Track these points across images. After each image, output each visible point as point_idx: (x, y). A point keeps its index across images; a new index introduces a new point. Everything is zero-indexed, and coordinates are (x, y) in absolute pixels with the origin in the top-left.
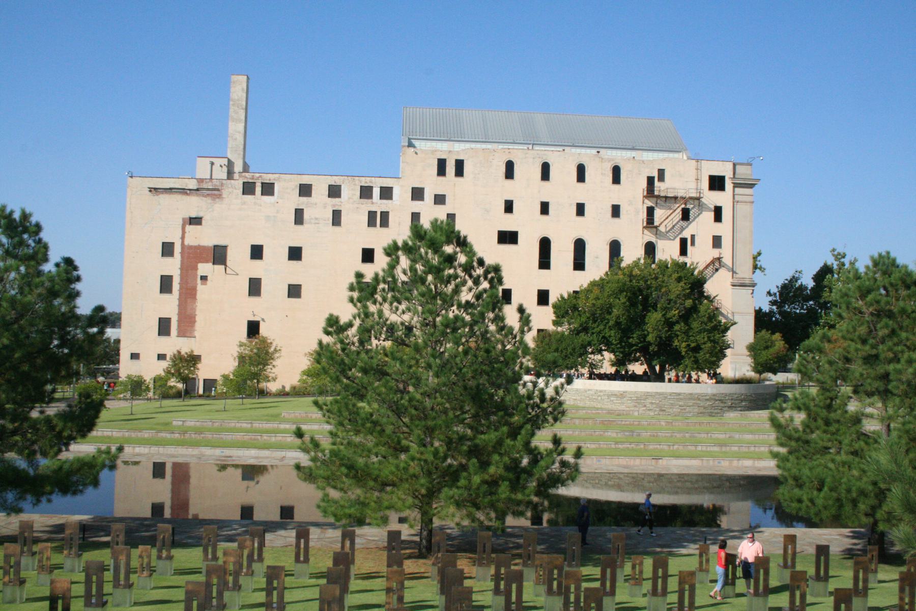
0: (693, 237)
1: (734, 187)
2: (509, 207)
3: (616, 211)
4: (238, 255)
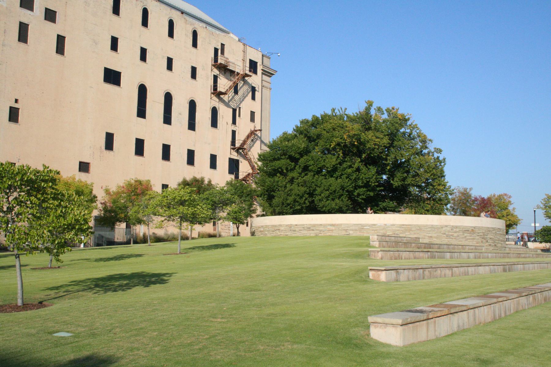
1: (263, 74)
2: (114, 44)
3: (194, 74)
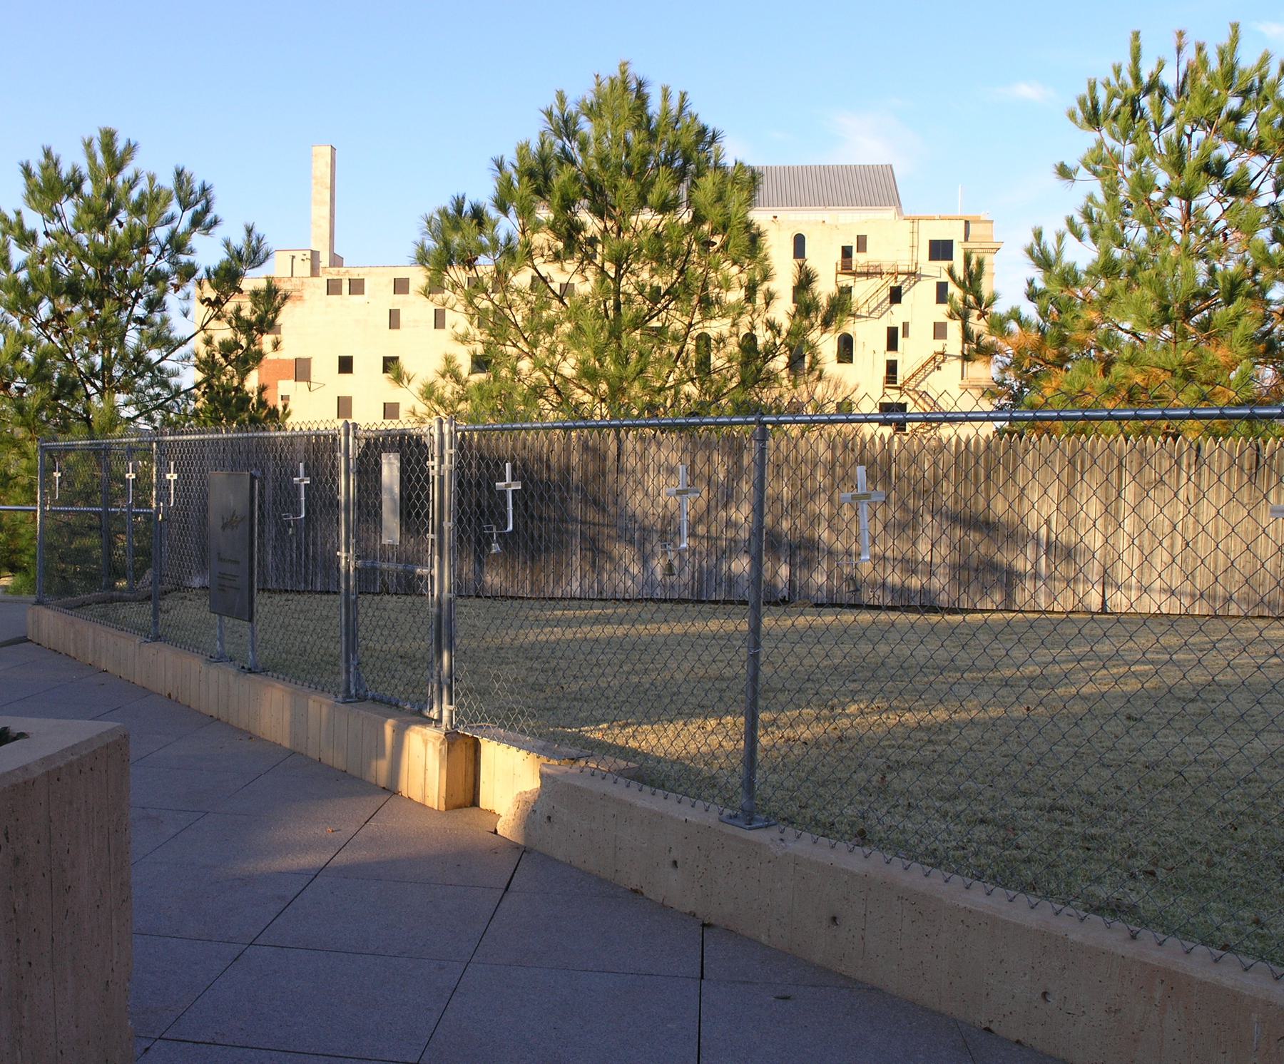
0: (905, 325)
4: (324, 368)
